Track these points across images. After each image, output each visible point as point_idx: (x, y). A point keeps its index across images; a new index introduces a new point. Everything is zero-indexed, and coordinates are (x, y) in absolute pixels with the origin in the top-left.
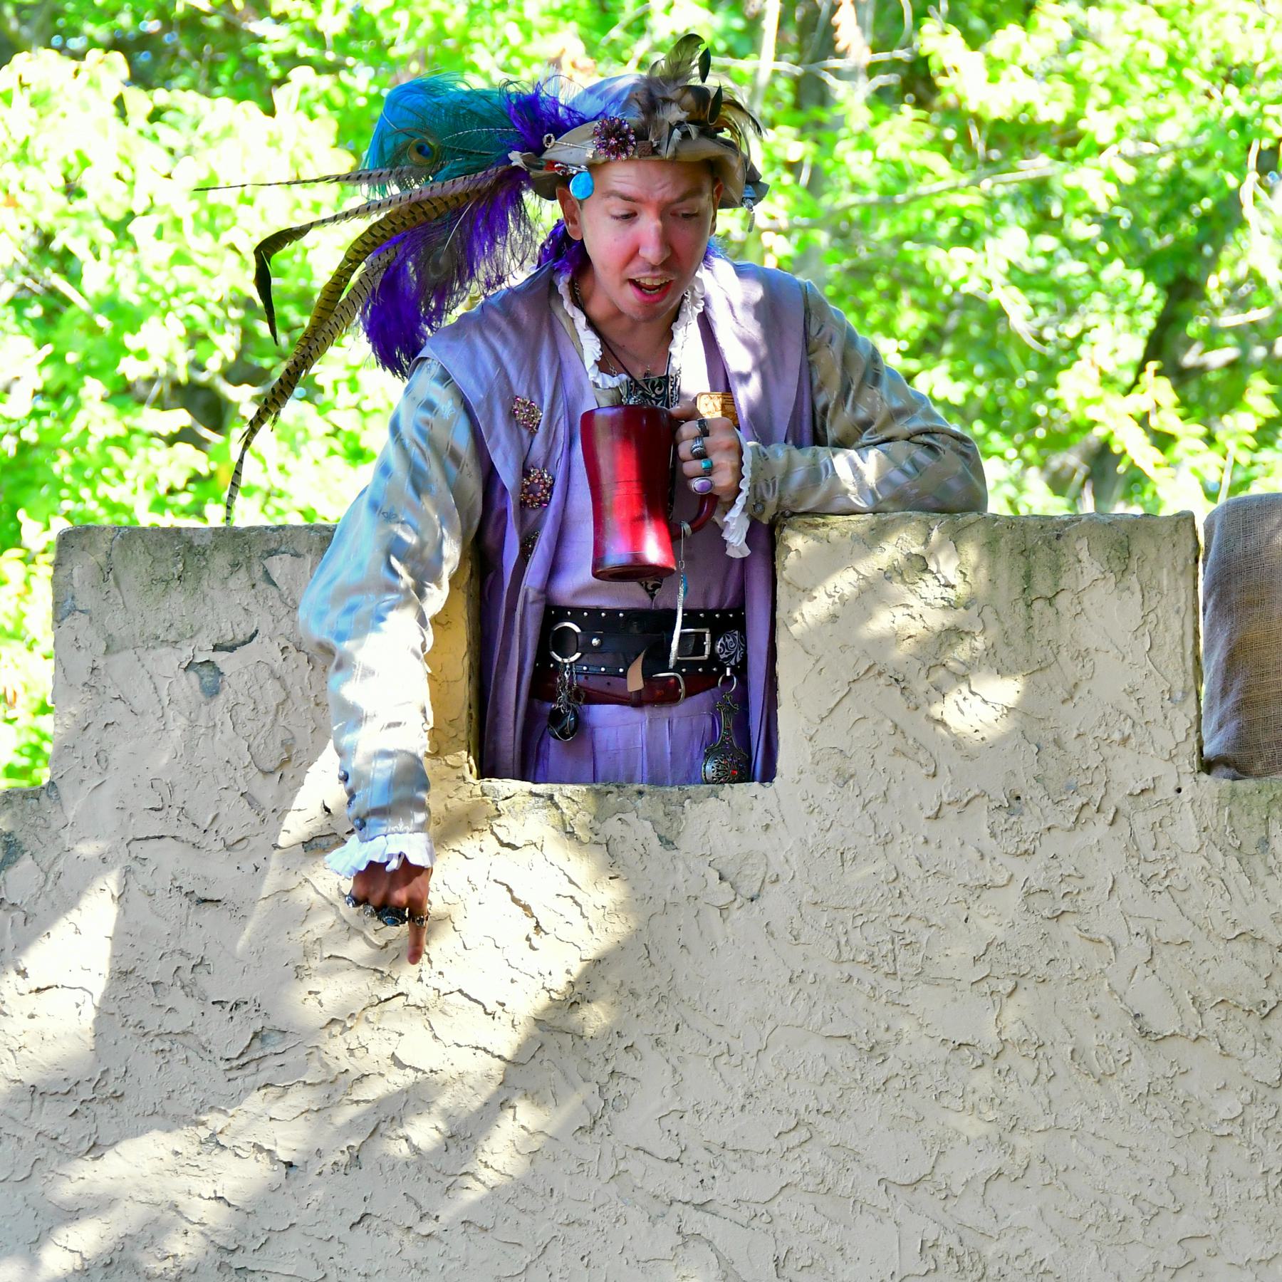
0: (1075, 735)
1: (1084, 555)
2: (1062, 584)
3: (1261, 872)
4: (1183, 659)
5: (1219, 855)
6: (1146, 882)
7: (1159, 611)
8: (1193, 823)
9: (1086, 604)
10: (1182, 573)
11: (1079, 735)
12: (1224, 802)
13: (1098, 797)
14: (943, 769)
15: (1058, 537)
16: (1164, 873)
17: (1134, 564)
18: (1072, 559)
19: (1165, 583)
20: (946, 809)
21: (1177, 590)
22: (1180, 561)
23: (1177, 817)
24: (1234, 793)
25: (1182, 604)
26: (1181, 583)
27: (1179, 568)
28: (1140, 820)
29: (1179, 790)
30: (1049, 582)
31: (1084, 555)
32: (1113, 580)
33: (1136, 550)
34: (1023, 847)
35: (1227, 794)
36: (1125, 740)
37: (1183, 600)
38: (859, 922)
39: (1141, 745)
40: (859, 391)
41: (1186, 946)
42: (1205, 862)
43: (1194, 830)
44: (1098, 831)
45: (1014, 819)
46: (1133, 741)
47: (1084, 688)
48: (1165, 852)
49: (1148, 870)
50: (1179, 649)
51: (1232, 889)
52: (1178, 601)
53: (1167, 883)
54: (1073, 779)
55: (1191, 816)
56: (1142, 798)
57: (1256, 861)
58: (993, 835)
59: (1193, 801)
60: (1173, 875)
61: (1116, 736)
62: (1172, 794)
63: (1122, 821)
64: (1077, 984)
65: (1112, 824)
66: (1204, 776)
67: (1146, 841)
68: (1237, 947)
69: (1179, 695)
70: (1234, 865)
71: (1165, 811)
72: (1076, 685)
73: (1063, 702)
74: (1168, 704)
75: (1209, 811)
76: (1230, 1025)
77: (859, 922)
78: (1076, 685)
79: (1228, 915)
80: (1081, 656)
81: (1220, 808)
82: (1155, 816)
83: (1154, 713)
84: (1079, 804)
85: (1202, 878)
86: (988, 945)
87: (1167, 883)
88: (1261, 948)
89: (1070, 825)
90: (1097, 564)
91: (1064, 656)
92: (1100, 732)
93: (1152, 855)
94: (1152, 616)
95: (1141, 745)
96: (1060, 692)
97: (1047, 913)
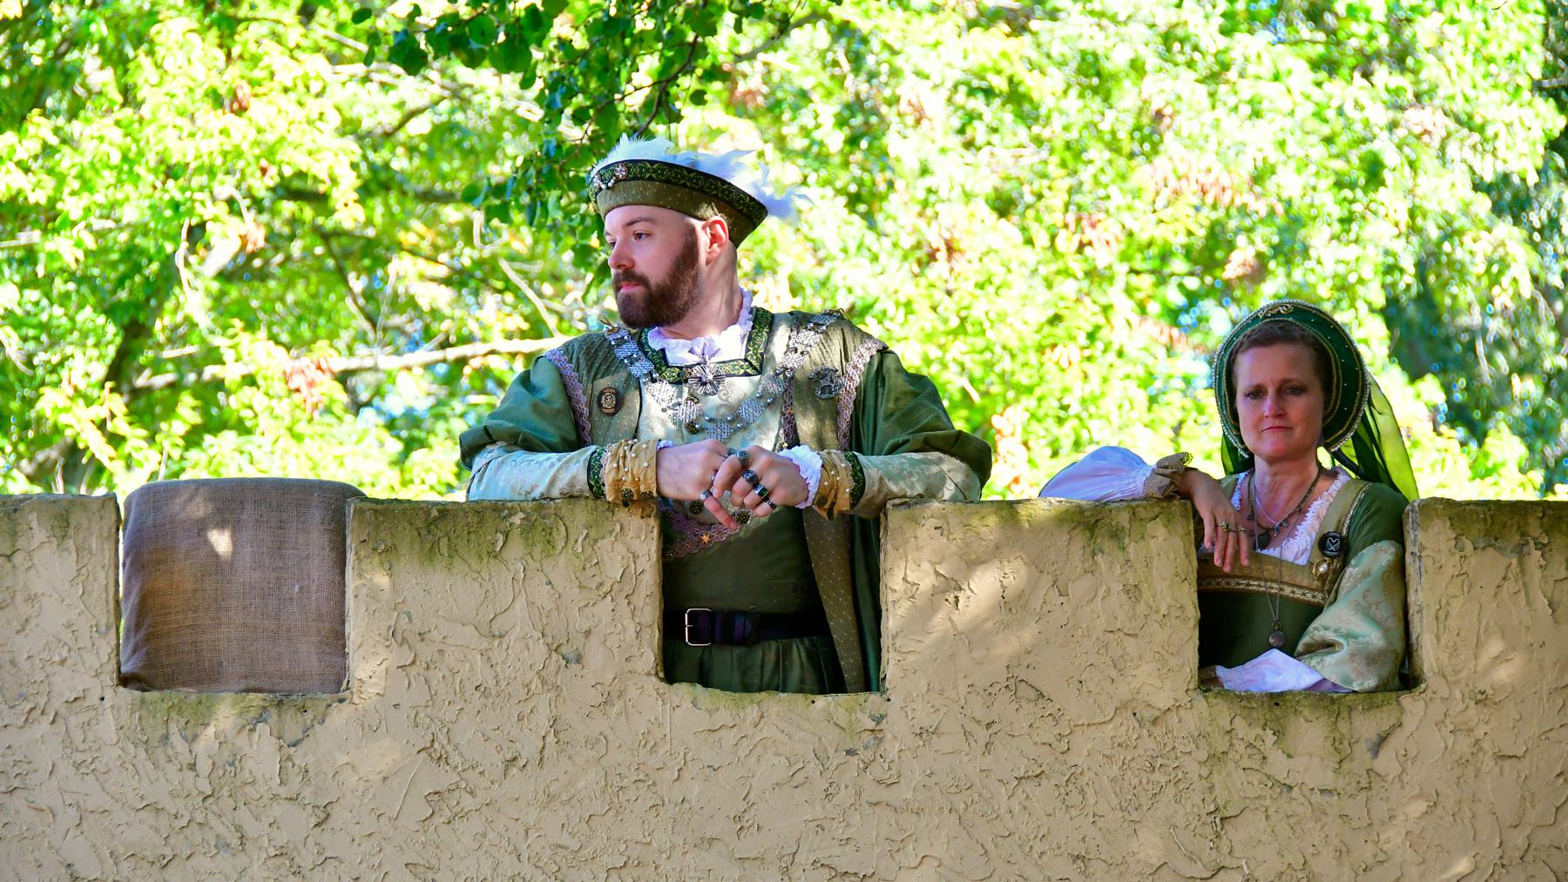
1: (34, 524)
2: (18, 545)
3: (162, 760)
5: (132, 746)
6: (77, 766)
7: (90, 567)
9: (36, 561)
10: (107, 539)
12: (136, 708)
13: (42, 702)
15: (15, 510)
17: (71, 532)
18: (25, 527)
21: (103, 551)
22: (106, 529)
24: (143, 701)
26: (106, 546)
27: (105, 535)
28: (73, 721)
29: (103, 699)
30: (9, 544)
31: (34, 524)
32: (55, 543)
33: (73, 522)
35: (138, 702)
36: (63, 662)
39: (75, 664)
42: (120, 752)
46: (69, 662)
47: (33, 622)
49: (79, 757)
50: (104, 595)
51: (141, 772)
53: (92, 767)
54: (23, 690)
55: (111, 718)
56: (75, 704)
57: (159, 751)
59: (112, 707)
60: (97, 762)
61: (57, 658)
62: (97, 701)
63: (60, 721)
64: (25, 841)
65: (53, 722)
66: (121, 689)
67: (78, 736)
68: (143, 814)
69: (103, 628)
70: (142, 755)
71: (92, 714)
72: (27, 620)
73: (18, 632)
74: (96, 635)
75: (125, 715)
76: (138, 872)
78: (27, 620)
80: (31, 598)
81: (133, 712)
82: (84, 717)
83: (85, 641)
84: (28, 707)
88: (163, 816)
89: (21, 723)
90: (44, 531)
91: (19, 598)
92: (45, 656)
93: (82, 747)
94: (84, 570)
95: (75, 664)
96: (16, 625)
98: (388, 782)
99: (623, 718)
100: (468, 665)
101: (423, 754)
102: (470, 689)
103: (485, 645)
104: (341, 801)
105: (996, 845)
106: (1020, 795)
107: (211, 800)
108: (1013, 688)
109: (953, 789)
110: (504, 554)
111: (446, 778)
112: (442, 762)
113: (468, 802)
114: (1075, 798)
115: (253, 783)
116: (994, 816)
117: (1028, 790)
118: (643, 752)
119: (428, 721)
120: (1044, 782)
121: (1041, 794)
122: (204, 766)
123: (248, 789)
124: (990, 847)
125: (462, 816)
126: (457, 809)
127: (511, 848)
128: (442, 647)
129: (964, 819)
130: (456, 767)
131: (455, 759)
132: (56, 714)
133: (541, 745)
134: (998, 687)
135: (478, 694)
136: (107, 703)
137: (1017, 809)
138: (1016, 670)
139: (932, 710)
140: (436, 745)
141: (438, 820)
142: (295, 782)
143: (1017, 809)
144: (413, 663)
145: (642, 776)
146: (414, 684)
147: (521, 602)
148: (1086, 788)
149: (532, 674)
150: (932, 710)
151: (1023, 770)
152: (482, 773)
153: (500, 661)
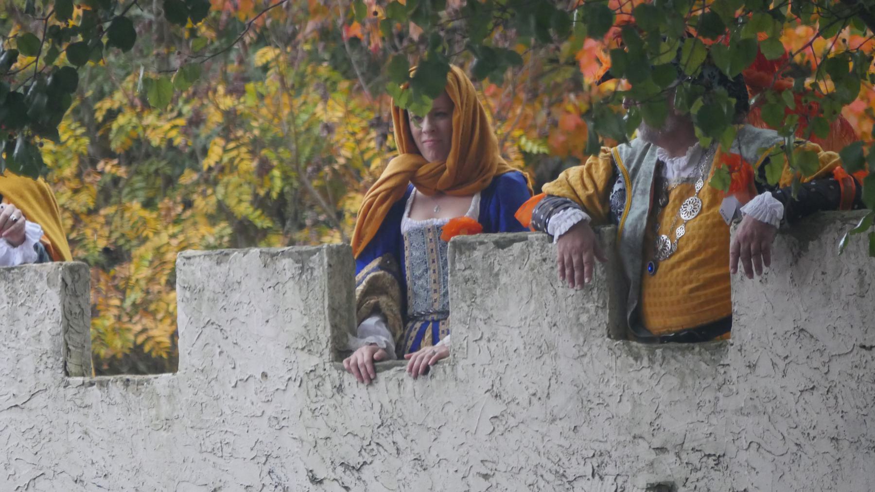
14: (237, 366)
20: (239, 383)
38: (208, 434)
40: (453, 263)
49: (313, 407)
53: (321, 412)
58: (256, 394)
60: (323, 408)
77: (208, 434)
86: (256, 442)
87: (321, 412)
99: (590, 365)
101: (488, 394)
102: (511, 353)
105: (789, 434)
106: (802, 402)
108: (797, 334)
109: (766, 400)
112: (498, 398)
113: (512, 422)
114: (832, 402)
116: (788, 415)
117: (806, 398)
118: (602, 386)
119: (490, 373)
120: (815, 392)
121: (814, 399)
124: (786, 435)
125: (508, 430)
126: (506, 426)
127: (534, 448)
129: (772, 417)
130: (505, 401)
131: (505, 396)
133: (548, 385)
134: (789, 334)
135: (516, 355)
137: (800, 410)
138: (799, 322)
139: (754, 351)
140: (495, 388)
141: (497, 433)
143: (800, 410)
145: (601, 401)
148: (838, 395)
150: (754, 351)
151: (803, 386)
152: (518, 404)
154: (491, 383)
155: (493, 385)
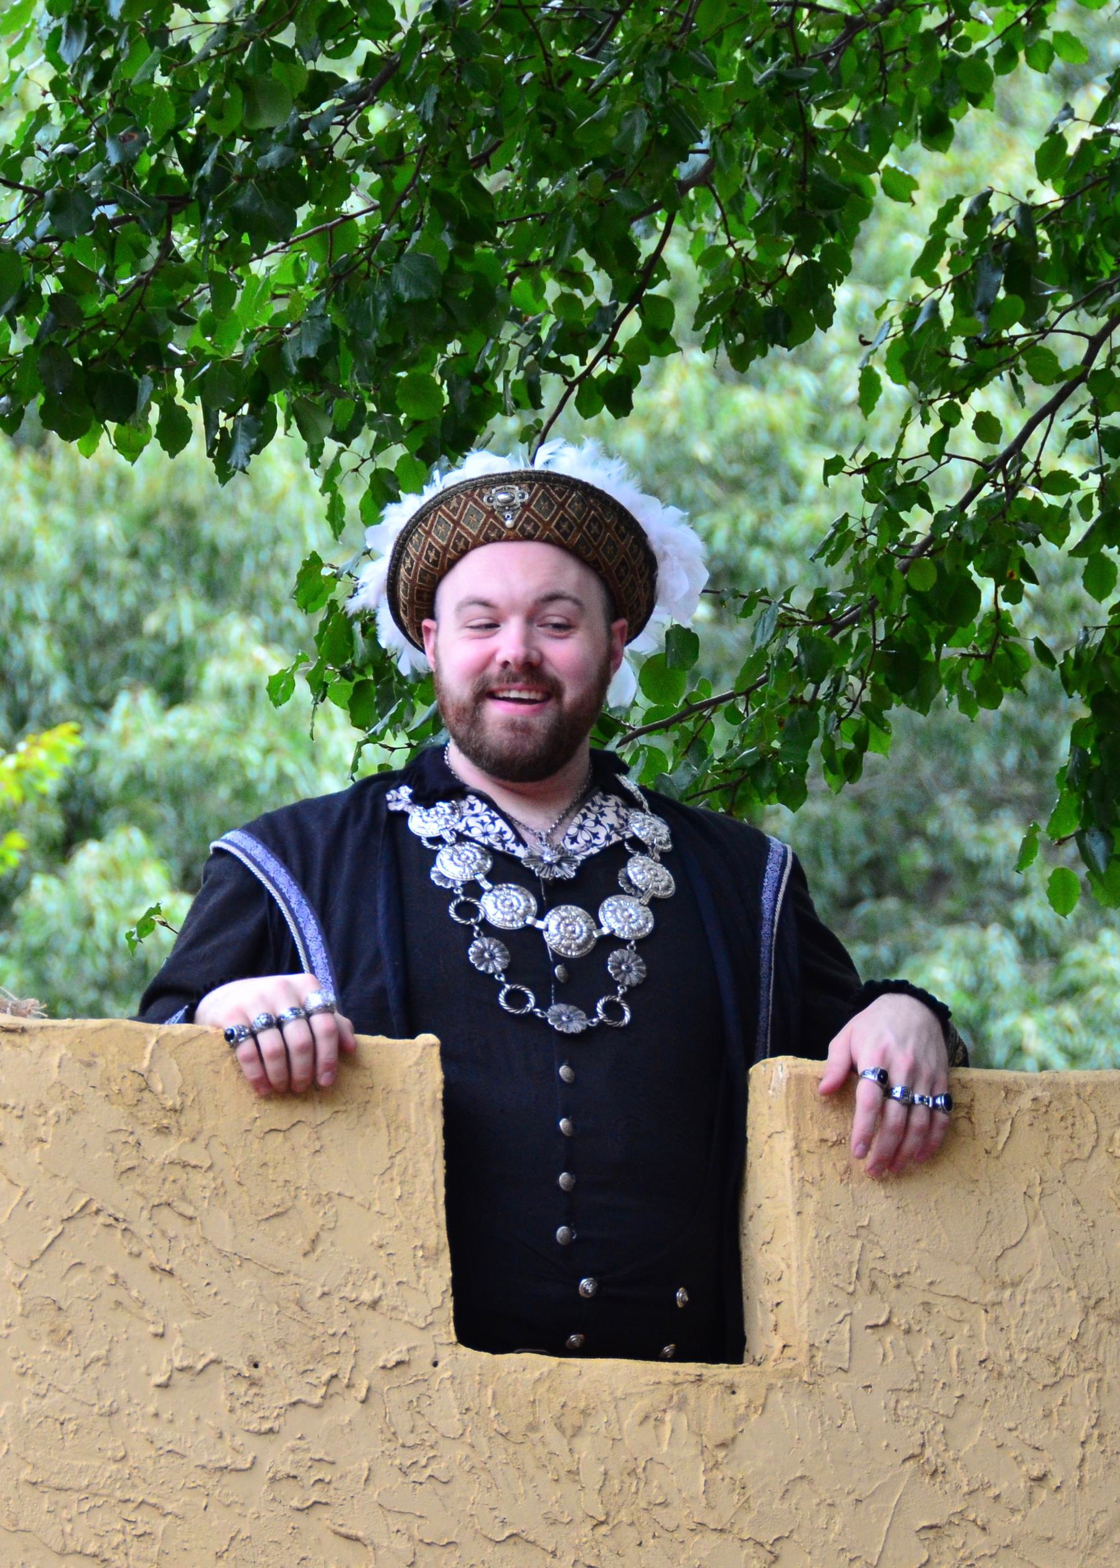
0: (319, 1292)
4: (435, 1207)
8: (454, 1404)
11: (324, 1294)
16: (423, 1462)
19: (413, 1120)
23: (435, 1396)
25: (431, 1144)
27: (428, 1103)
29: (435, 1364)
34: (266, 1426)
37: (433, 1140)
41: (451, 1548)
43: (456, 1411)
44: (347, 1409)
45: (254, 1390)
46: (384, 1303)
48: (425, 1437)
49: (404, 1458)
50: (431, 1198)
52: (428, 1140)
53: (428, 1472)
55: (451, 1395)
61: (366, 1296)
66: (463, 1349)
67: (403, 1421)
71: (422, 1388)
79: (496, 1513)
82: (411, 1394)
84: (325, 1377)
85: (467, 1468)
87: (428, 1472)
92: (347, 1292)
93: (411, 1440)
96: (301, 1242)
97: (295, 1503)
98: (862, 1506)
100: (966, 1329)
103: (990, 1297)
104: (795, 1537)
107: (604, 1529)
110: (1008, 1157)
111: (942, 1509)
113: (979, 1543)
115: (664, 1504)
122: (591, 1477)
123: (659, 1513)
128: (929, 1298)
130: (959, 1487)
132: (369, 1390)
136: (444, 1372)
140: (928, 1452)
142: (728, 1503)
144: (888, 1322)
146: (890, 1358)
147: (1038, 1232)
149: (1059, 1344)
153: (1013, 1322)
154: (917, 1439)
155: (923, 1445)
